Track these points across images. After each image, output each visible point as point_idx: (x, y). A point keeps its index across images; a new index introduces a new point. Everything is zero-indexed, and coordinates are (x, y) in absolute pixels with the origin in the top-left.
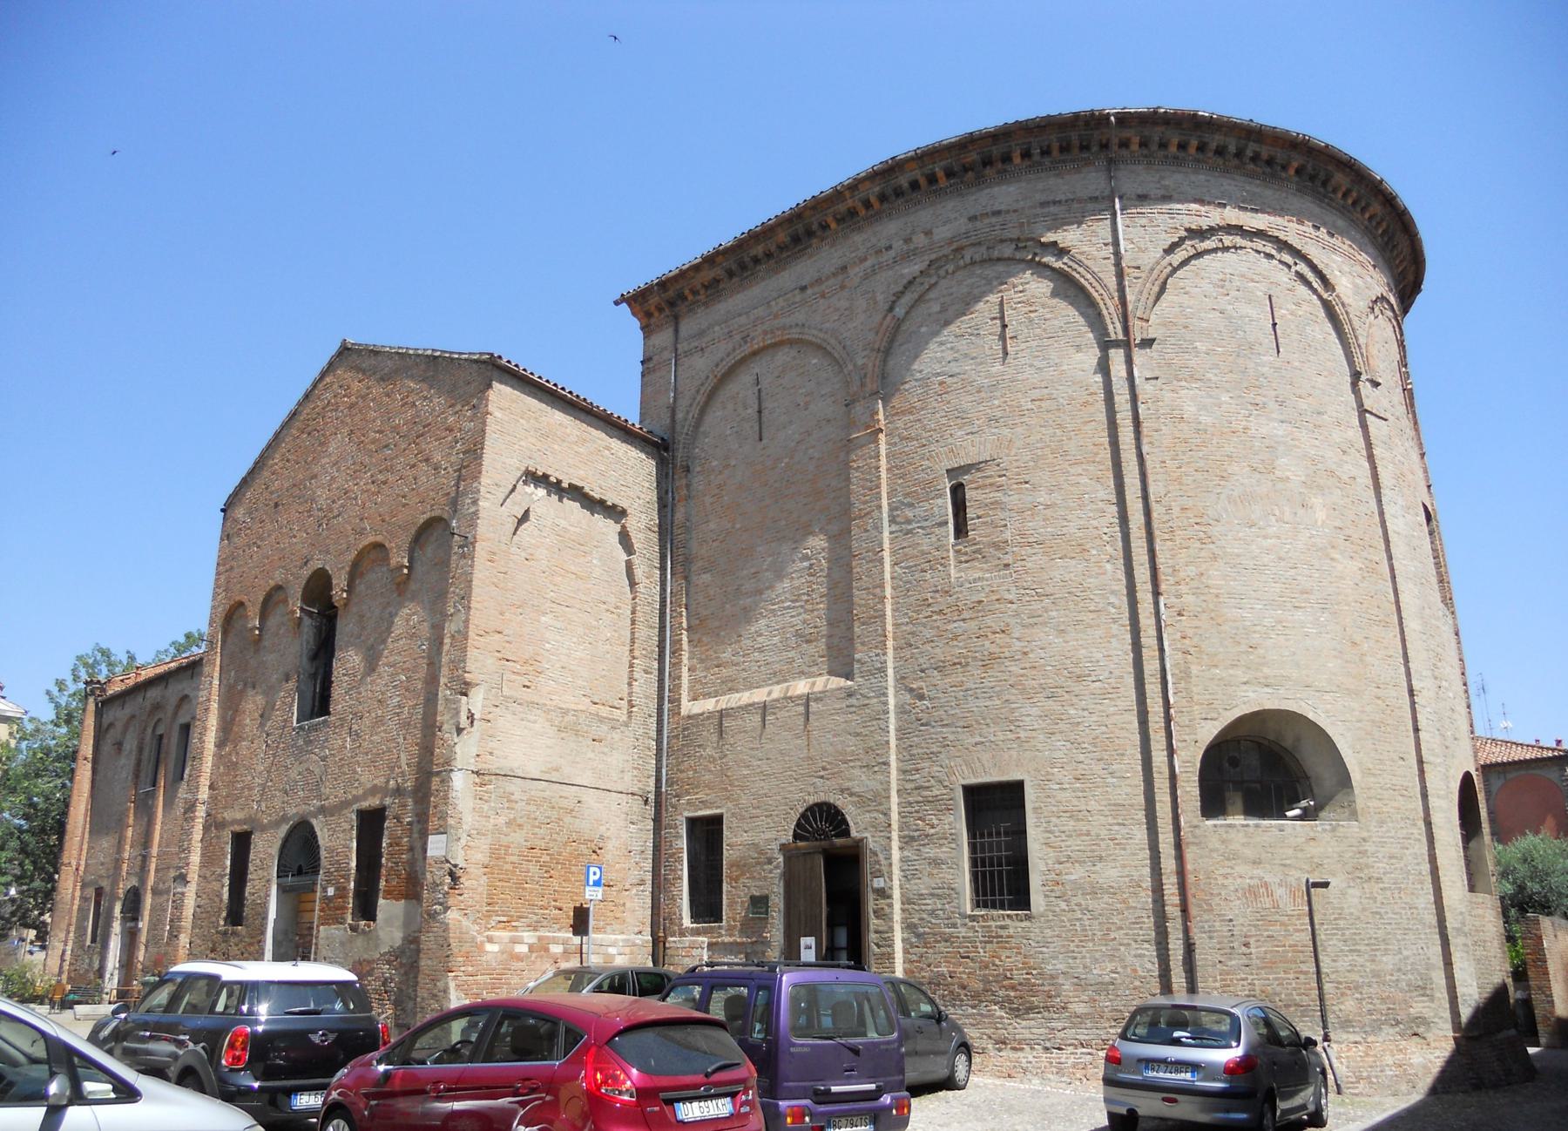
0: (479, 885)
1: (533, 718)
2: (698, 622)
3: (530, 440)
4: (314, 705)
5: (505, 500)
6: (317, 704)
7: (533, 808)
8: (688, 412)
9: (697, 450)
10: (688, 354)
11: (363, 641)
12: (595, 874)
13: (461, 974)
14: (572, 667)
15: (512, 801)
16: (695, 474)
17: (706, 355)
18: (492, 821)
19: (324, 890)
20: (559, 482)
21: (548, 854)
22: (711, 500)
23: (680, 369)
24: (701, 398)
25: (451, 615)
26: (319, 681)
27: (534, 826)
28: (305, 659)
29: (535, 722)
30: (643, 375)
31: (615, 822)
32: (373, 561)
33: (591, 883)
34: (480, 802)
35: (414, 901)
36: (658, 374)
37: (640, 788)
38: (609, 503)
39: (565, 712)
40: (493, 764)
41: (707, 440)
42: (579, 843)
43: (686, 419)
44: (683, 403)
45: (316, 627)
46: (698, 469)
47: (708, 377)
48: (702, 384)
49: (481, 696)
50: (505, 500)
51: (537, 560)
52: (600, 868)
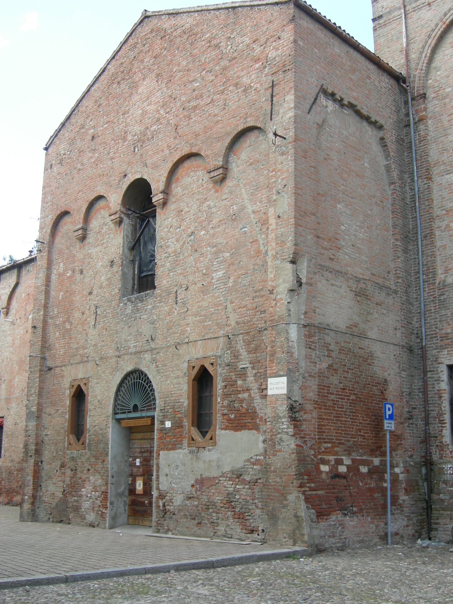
0: (312, 417)
1: (339, 284)
2: (444, 212)
3: (322, 64)
4: (134, 284)
5: (311, 108)
6: (136, 283)
7: (343, 357)
8: (421, 53)
9: (430, 81)
10: (417, 9)
11: (183, 230)
12: (389, 409)
13: (308, 489)
14: (358, 245)
15: (330, 350)
16: (430, 99)
17: (433, 7)
18: (318, 366)
19: (163, 423)
20: (342, 99)
21: (354, 394)
22: (448, 118)
23: (409, 21)
24: (432, 42)
25: (275, 201)
26: (136, 266)
27: (344, 371)
28: (126, 250)
29: (340, 287)
30: (375, 30)
31: (393, 369)
32: (189, 168)
33: (387, 417)
34: (309, 350)
35: (254, 431)
36: (390, 27)
37: (406, 343)
38: (373, 120)
39: (358, 280)
40: (317, 319)
41: (438, 73)
42: (373, 385)
43: (420, 58)
44: (416, 47)
45: (132, 225)
46: (433, 95)
47: (437, 25)
48: (433, 30)
49: (305, 264)
50: (311, 108)
51: (331, 160)
52: (392, 405)
